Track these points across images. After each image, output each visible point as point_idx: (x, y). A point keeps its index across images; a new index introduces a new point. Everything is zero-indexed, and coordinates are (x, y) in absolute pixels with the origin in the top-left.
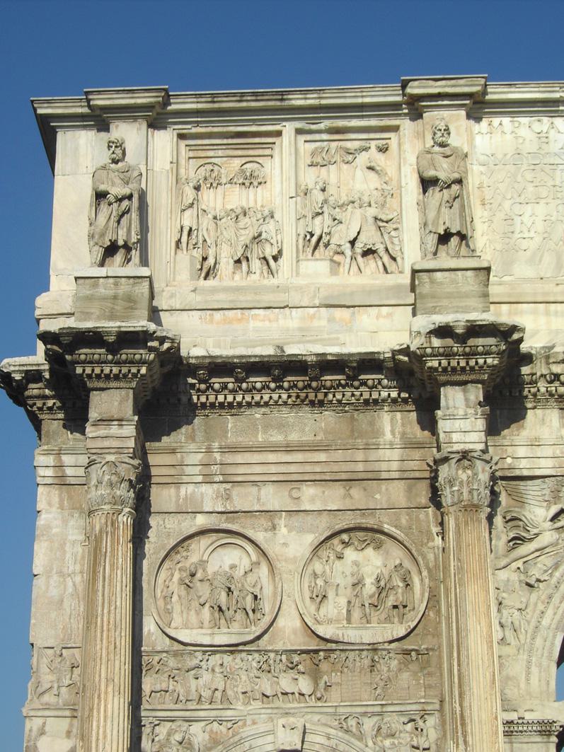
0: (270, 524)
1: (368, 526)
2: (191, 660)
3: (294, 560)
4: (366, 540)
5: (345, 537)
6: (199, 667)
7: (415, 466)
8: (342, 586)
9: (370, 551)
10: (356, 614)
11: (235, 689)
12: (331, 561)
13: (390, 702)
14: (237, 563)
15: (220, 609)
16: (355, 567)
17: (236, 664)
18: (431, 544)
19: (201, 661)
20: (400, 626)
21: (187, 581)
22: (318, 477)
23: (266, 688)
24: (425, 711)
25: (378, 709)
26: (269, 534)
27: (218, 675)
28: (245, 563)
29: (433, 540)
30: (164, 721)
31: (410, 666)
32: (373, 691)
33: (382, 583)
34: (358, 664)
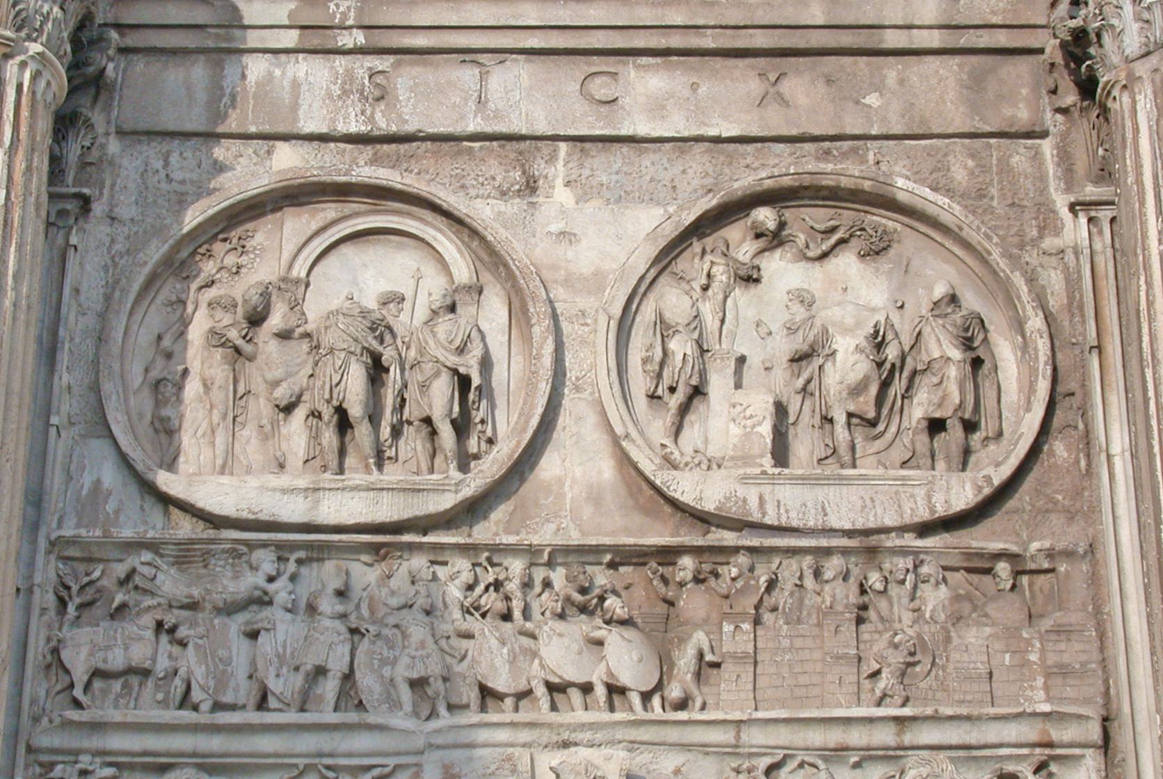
0: (518, 174)
1: (845, 182)
2: (236, 576)
3: (596, 283)
4: (833, 230)
5: (765, 216)
6: (264, 601)
7: (993, 13)
8: (754, 361)
9: (847, 263)
10: (804, 446)
11: (387, 671)
12: (716, 287)
13: (929, 711)
14: (407, 290)
15: (344, 423)
16: (800, 313)
17: (393, 593)
18: (1049, 243)
19: (271, 579)
20: (955, 478)
21: (233, 334)
22: (676, 41)
23: (492, 666)
24: (1050, 745)
25: (885, 736)
26: (514, 207)
27: (327, 623)
28: (433, 287)
29: (1058, 232)
30: (131, 767)
31: (991, 609)
32: (866, 684)
33: (891, 353)
34: (810, 600)
